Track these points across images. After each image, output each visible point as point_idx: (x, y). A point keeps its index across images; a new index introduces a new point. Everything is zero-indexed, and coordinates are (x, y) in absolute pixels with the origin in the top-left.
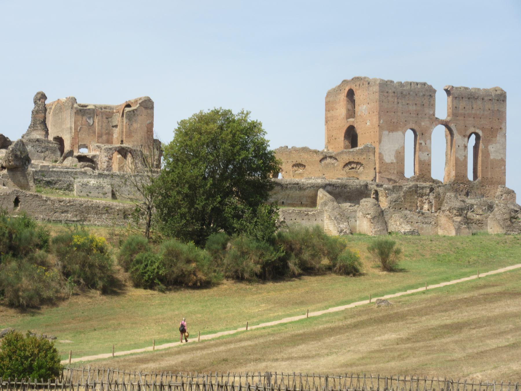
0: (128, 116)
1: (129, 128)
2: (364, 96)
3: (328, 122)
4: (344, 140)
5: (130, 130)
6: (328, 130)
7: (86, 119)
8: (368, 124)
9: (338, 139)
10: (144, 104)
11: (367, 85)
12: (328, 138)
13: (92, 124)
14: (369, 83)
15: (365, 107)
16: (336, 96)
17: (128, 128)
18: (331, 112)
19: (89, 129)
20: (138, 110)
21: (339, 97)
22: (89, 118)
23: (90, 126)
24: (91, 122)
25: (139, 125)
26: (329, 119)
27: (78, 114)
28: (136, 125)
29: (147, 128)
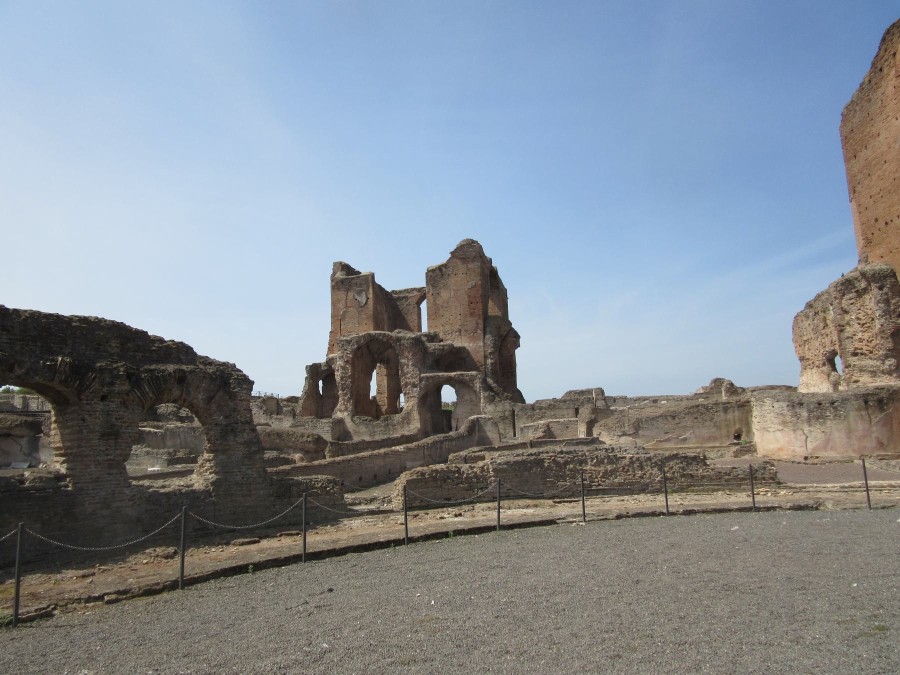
0: (430, 280)
1: (434, 301)
3: (859, 188)
5: (435, 305)
6: (861, 210)
7: (354, 296)
10: (461, 253)
12: (864, 233)
13: (364, 302)
17: (432, 301)
18: (863, 154)
19: (359, 313)
20: (449, 265)
22: (359, 293)
23: (362, 307)
24: (363, 299)
25: (452, 294)
27: (339, 289)
28: (445, 295)
29: (469, 296)
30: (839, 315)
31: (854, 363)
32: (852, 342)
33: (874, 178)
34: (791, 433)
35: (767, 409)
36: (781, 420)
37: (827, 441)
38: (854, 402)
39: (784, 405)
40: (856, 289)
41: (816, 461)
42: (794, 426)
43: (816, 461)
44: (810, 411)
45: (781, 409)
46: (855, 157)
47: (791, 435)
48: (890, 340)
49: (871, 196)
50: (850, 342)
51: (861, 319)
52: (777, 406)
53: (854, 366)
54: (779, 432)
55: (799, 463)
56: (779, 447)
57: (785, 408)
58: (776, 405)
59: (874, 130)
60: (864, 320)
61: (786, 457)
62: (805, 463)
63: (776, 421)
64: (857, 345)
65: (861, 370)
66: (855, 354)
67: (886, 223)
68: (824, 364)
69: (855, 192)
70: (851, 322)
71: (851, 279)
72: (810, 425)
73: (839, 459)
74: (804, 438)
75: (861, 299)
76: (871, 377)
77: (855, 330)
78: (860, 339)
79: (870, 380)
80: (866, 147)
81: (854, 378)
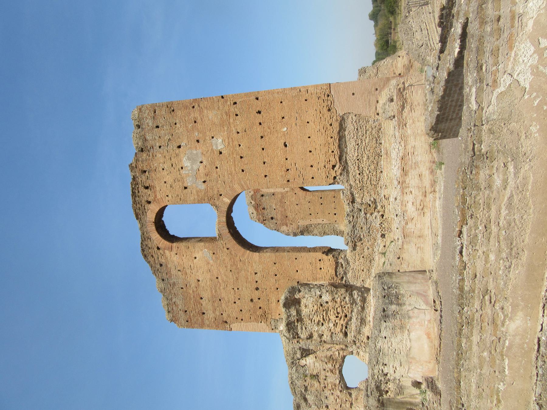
2: (166, 167)
4: (259, 252)
8: (219, 143)
9: (258, 277)
11: (144, 155)
12: (256, 320)
14: (142, 150)
15: (186, 163)
16: (174, 284)
21: (173, 272)
26: (218, 313)
30: (312, 342)
31: (353, 336)
32: (336, 334)
33: (223, 295)
34: (411, 321)
35: (387, 347)
36: (398, 330)
37: (418, 294)
38: (385, 279)
39: (384, 324)
40: (296, 321)
41: (438, 302)
42: (405, 318)
43: (438, 302)
44: (391, 303)
45: (388, 329)
46: (204, 313)
47: (414, 322)
48: (339, 290)
49: (235, 303)
50: (335, 335)
51: (319, 321)
52: (384, 333)
53: (354, 336)
54: (411, 334)
55: (441, 316)
56: (426, 337)
57: (387, 324)
58: (383, 334)
59: (193, 285)
60: (320, 316)
61: (436, 329)
62: (441, 311)
63: (399, 337)
64: (338, 329)
65: (359, 332)
66: (346, 334)
67: (257, 289)
68: (350, 394)
69: (226, 322)
70: (320, 332)
71: (287, 322)
72: (404, 304)
73: (434, 287)
74: (416, 311)
75: (304, 320)
76: (365, 326)
77: (327, 329)
78: (334, 325)
79: (368, 327)
80: (202, 298)
81: (365, 340)
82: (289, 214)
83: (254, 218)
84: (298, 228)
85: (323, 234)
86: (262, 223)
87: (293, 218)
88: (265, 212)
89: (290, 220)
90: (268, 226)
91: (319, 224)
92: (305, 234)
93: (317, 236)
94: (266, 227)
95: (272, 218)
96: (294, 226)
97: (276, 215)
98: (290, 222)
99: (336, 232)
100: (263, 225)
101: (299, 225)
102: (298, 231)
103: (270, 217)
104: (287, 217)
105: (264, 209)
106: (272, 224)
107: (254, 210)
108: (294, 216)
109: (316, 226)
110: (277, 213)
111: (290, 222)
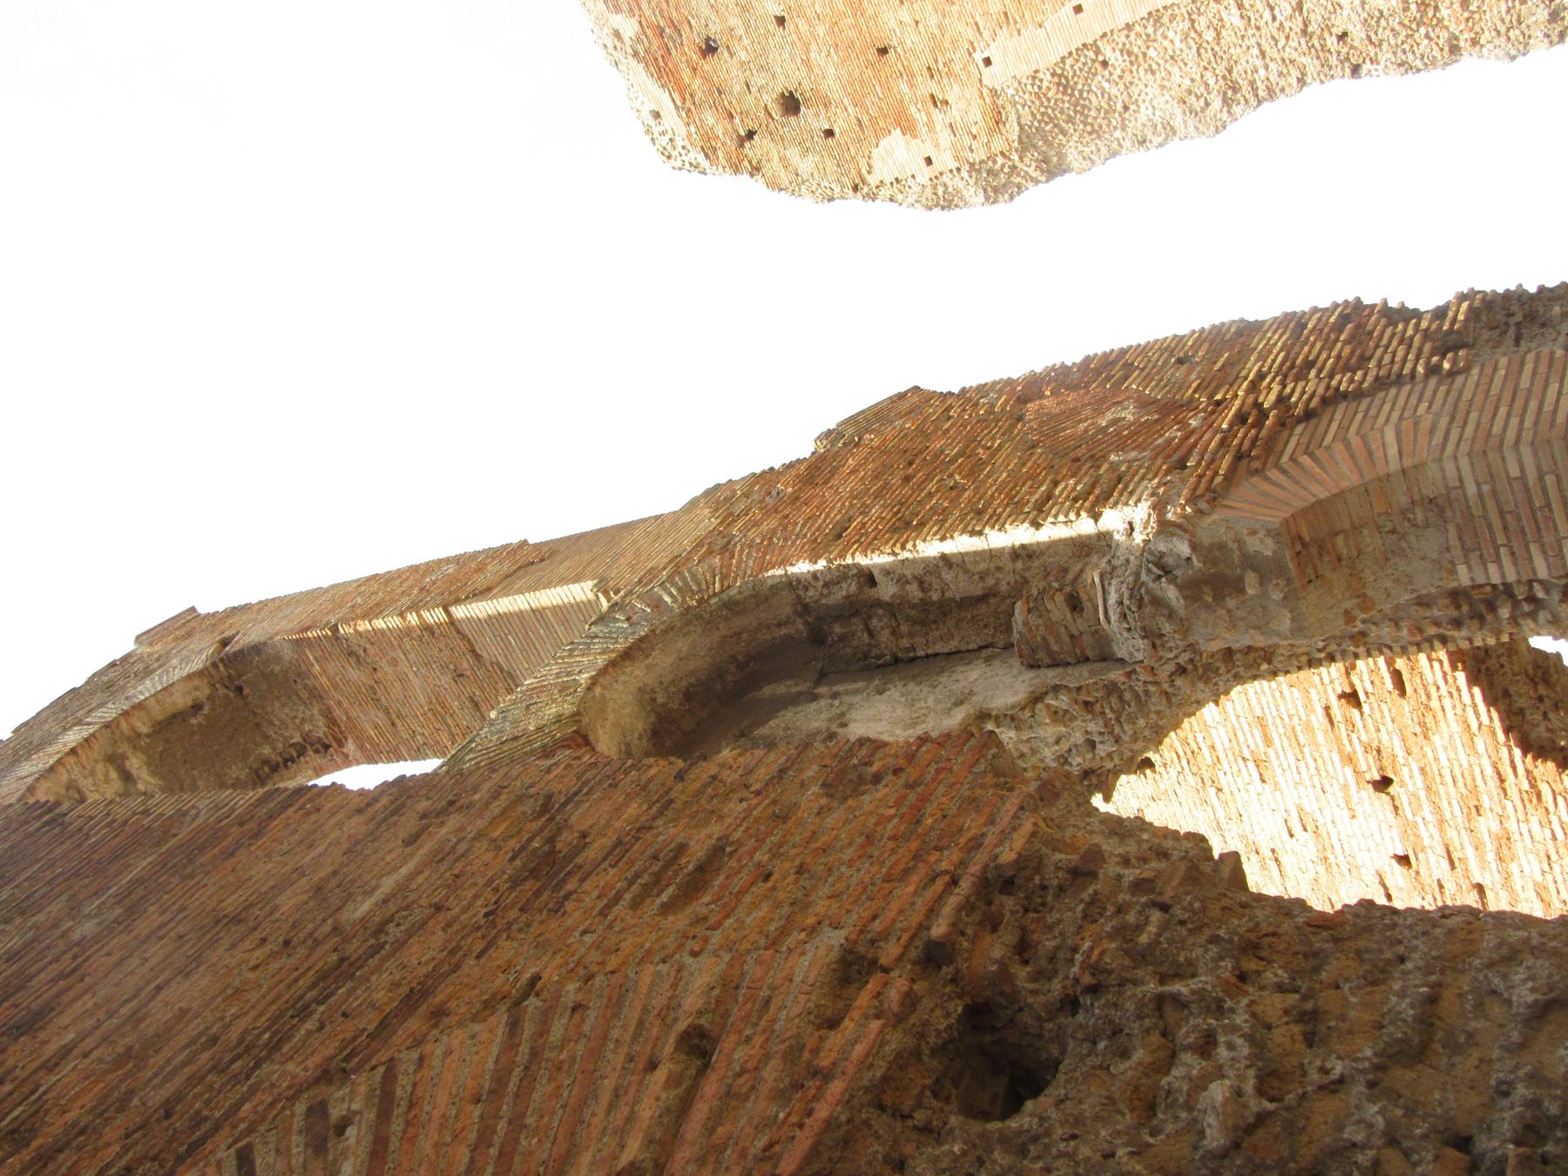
82: (892, 22)
83: (679, 143)
84: (997, 120)
85: (1217, 103)
86: (737, 170)
87: (936, 48)
88: (726, 68)
89: (915, 66)
90: (784, 178)
91: (1155, 17)
92: (1072, 156)
93: (1175, 144)
94: (774, 185)
95: (791, 104)
96: (965, 106)
97: (807, 63)
98: (927, 86)
99: (1332, 42)
100: (746, 177)
101: (994, 93)
102: (998, 144)
103: (770, 99)
104: (883, 51)
105: (709, 49)
106: (805, 152)
107: (652, 86)
108: (933, 21)
109: (1137, 45)
110: (808, 51)
111: (927, 86)
